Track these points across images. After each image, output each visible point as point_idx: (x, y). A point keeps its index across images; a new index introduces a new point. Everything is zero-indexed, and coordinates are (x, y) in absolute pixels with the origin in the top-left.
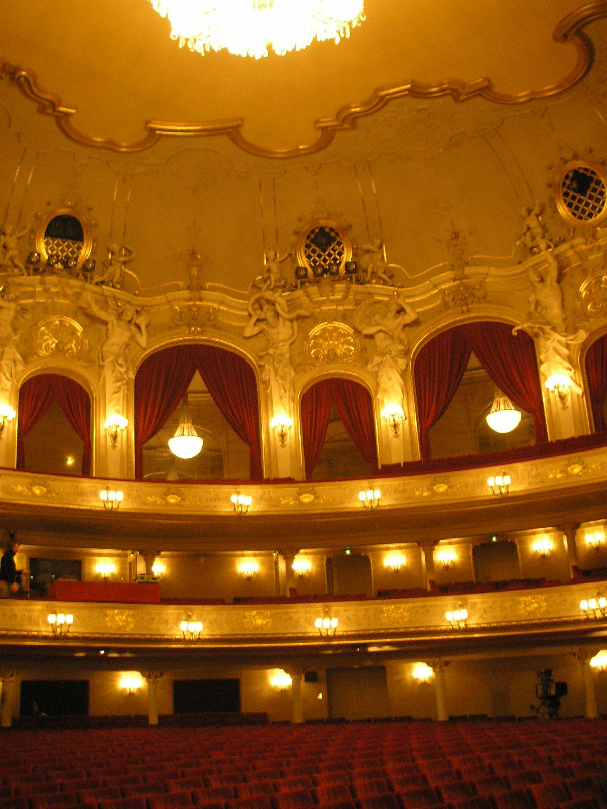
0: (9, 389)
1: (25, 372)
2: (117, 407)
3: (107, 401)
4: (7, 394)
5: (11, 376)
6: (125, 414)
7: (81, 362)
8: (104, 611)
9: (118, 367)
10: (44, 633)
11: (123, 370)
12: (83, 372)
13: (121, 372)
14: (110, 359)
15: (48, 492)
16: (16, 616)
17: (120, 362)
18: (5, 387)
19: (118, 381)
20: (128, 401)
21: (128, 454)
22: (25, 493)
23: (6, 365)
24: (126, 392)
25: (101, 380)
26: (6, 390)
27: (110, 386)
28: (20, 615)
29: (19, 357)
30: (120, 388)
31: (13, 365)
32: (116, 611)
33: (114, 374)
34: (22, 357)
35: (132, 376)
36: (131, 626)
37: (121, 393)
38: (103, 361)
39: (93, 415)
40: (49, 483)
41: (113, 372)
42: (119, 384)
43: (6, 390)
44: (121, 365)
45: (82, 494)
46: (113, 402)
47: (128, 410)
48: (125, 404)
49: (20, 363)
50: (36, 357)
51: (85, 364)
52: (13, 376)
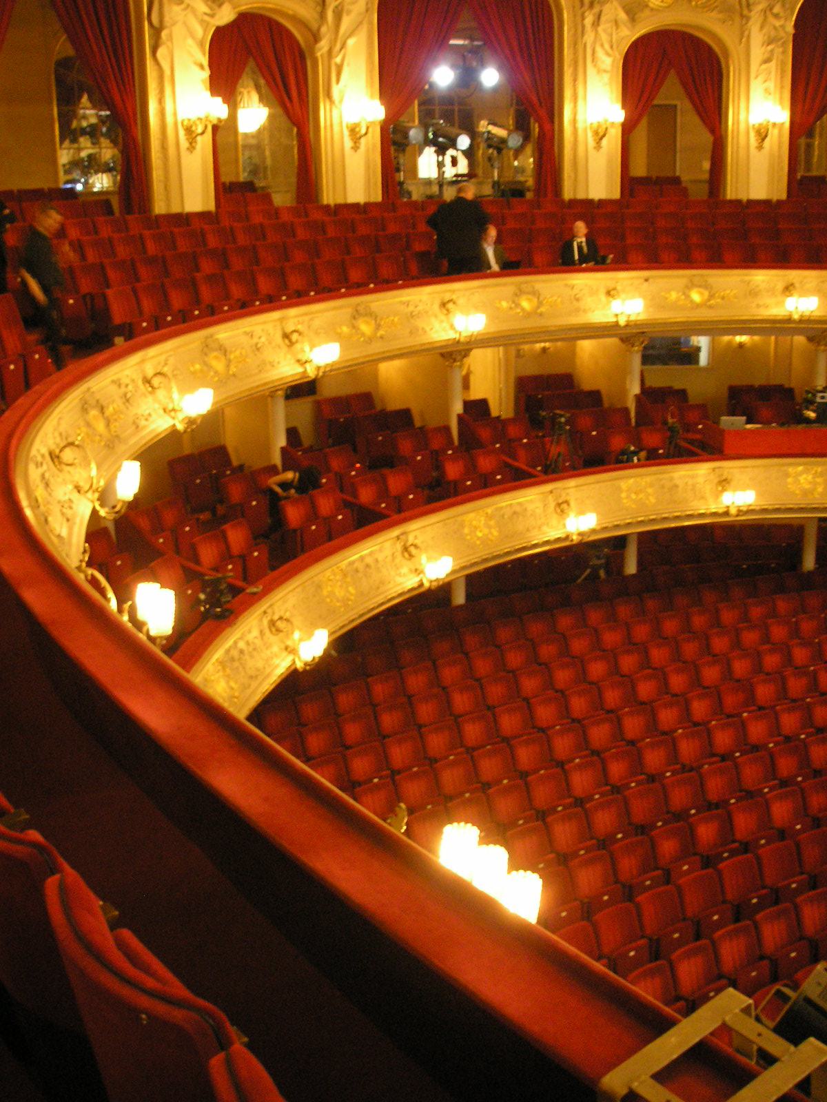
0: (609, 68)
1: (629, 35)
2: (767, 84)
3: (753, 75)
4: (606, 77)
5: (612, 47)
6: (777, 96)
7: (714, 14)
8: (785, 468)
9: (771, 19)
10: (714, 511)
11: (778, 23)
12: (719, 30)
13: (775, 28)
14: (760, 7)
15: (711, 296)
16: (676, 486)
17: (776, 10)
18: (603, 67)
19: (768, 44)
20: (783, 72)
21: (780, 156)
22: (681, 303)
23: (605, 31)
24: (781, 57)
25: (744, 40)
26: (605, 71)
27: (758, 51)
28: (680, 483)
29: (622, 15)
30: (772, 51)
31: (614, 28)
32: (800, 468)
33: (765, 30)
34: (628, 12)
35: (790, 28)
36: (820, 489)
37: (773, 64)
38: (750, 11)
39: (728, 98)
40: (711, 280)
41: (762, 27)
42: (770, 48)
43: (605, 71)
44: (777, 16)
45: (754, 293)
46: (761, 78)
47: (782, 87)
48: (779, 77)
49: (625, 26)
50: (647, 12)
51: (720, 16)
52: (614, 47)
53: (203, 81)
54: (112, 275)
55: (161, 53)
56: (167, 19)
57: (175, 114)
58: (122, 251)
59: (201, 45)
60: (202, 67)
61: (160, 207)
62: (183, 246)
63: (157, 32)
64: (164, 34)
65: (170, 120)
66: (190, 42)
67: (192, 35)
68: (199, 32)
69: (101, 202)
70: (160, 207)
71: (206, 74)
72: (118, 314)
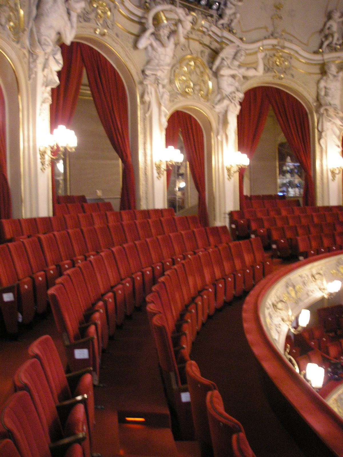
53: (339, 153)
54: (300, 231)
55: (322, 141)
56: (325, 128)
57: (327, 166)
58: (304, 221)
59: (338, 138)
60: (339, 147)
61: (319, 203)
62: (329, 219)
63: (320, 133)
64: (323, 134)
65: (325, 168)
66: (334, 136)
67: (335, 135)
68: (338, 132)
69: (295, 202)
70: (319, 203)
71: (340, 149)
72: (302, 247)
